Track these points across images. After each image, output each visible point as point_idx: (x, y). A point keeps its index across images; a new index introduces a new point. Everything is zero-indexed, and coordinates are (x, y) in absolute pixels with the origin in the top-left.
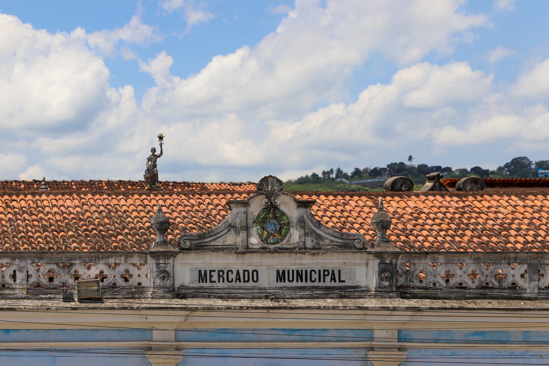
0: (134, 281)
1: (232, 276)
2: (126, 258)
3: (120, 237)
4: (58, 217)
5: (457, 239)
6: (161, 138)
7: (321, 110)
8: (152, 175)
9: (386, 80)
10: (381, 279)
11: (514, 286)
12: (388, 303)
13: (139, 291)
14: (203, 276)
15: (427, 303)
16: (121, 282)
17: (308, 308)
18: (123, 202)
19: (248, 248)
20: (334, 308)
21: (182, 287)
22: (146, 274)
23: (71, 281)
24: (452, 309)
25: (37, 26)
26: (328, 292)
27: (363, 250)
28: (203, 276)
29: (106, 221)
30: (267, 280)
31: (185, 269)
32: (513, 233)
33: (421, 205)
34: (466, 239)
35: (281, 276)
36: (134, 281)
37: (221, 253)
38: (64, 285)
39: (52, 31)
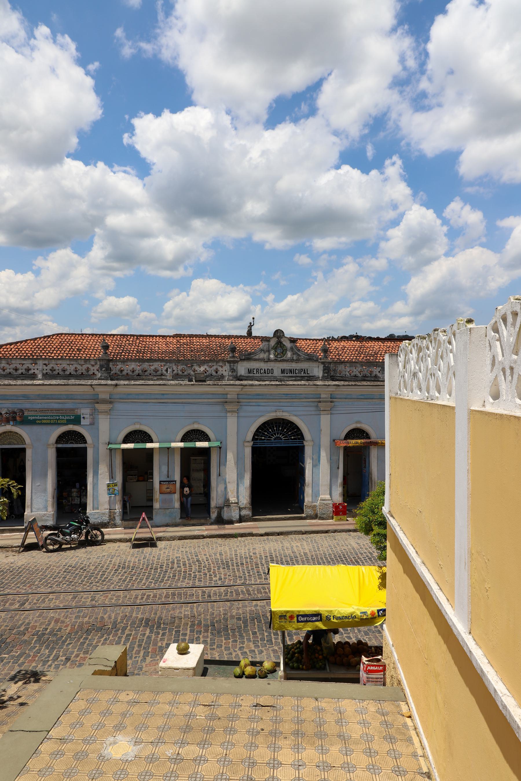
0: (220, 373)
1: (262, 371)
2: (217, 363)
3: (223, 355)
4: (198, 347)
5: (358, 358)
6: (253, 318)
7: (326, 315)
8: (250, 333)
9: (349, 306)
10: (324, 373)
11: (376, 376)
12: (327, 383)
13: (222, 377)
14: (250, 371)
15: (342, 383)
16: (214, 373)
17: (294, 385)
18: (227, 341)
19: (269, 359)
20: (304, 385)
21: (241, 376)
22: (225, 370)
23: (192, 373)
24: (352, 385)
25: (227, 284)
26: (302, 378)
27: (317, 361)
28: (250, 371)
29: (218, 348)
30: (277, 373)
31: (242, 369)
32: (379, 355)
33: (345, 345)
34: (361, 358)
35: (283, 371)
36: (220, 373)
37: (257, 362)
38: (189, 374)
39: (233, 286)
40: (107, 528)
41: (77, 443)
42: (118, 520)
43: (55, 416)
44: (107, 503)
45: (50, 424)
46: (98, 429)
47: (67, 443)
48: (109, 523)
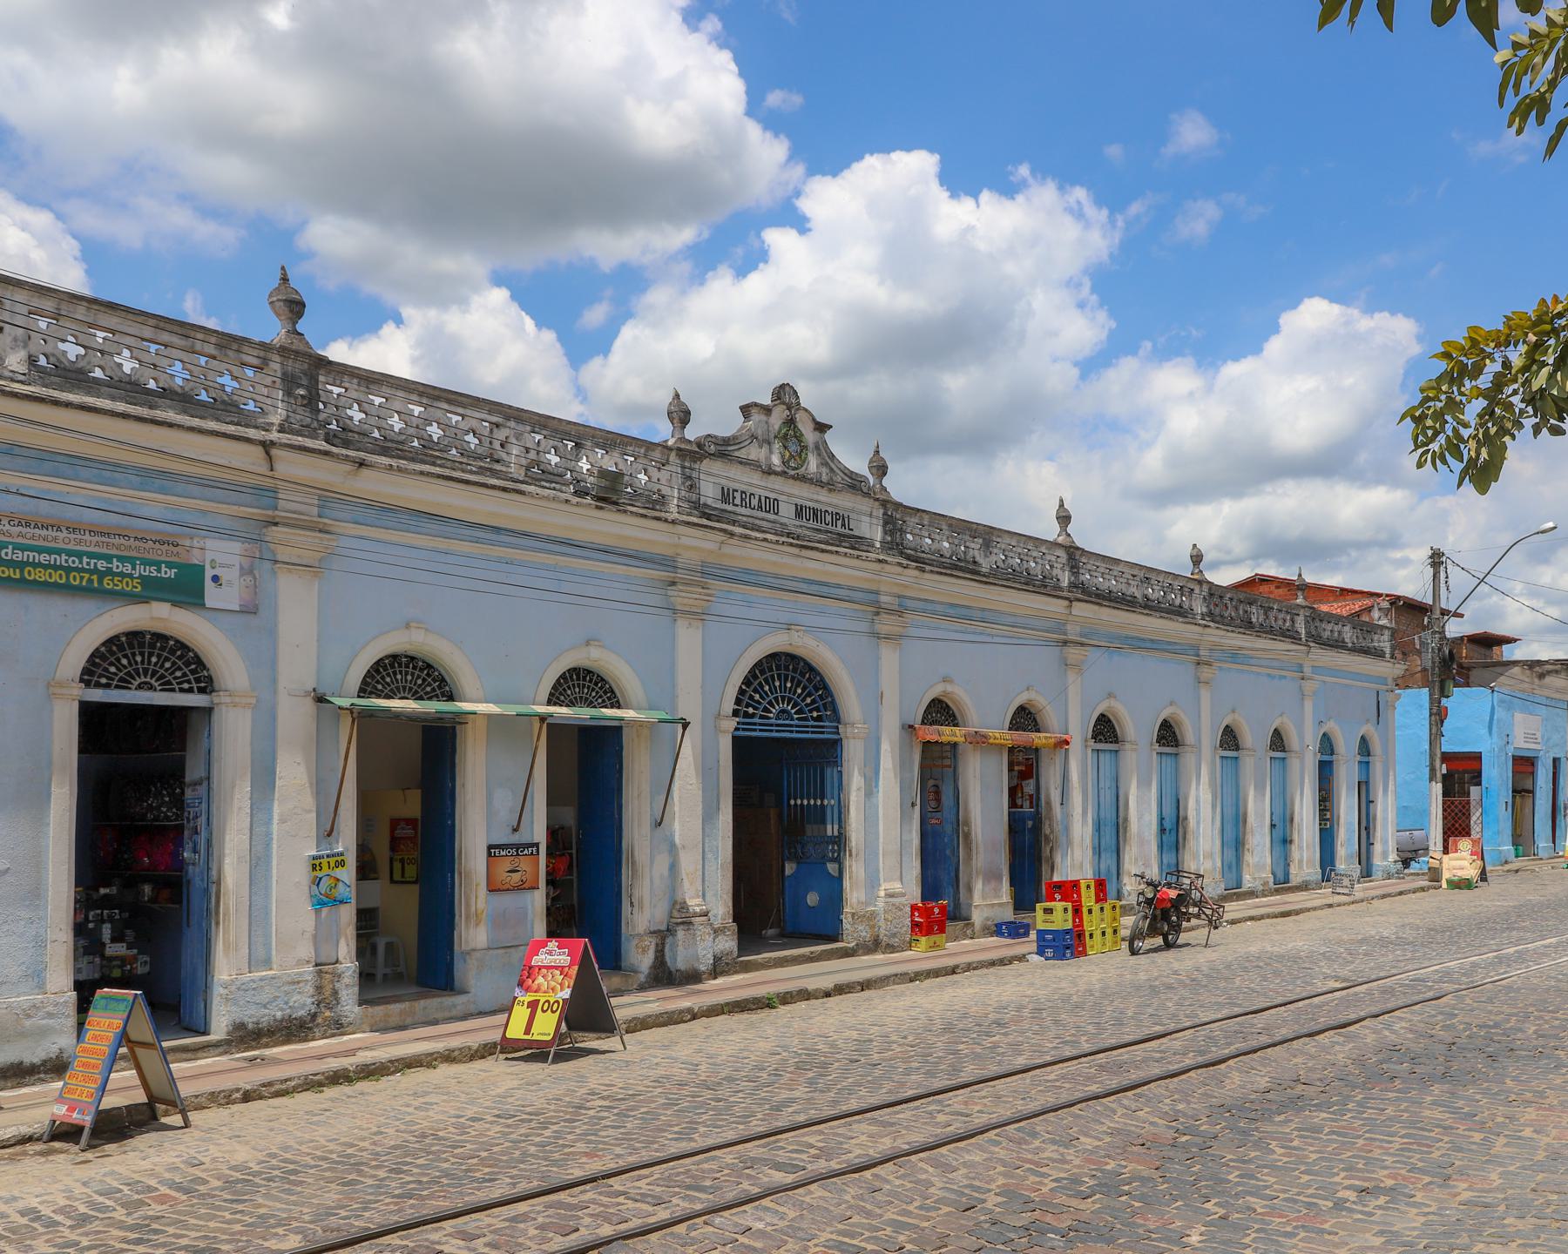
40: (306, 1040)
41: (167, 687)
42: (349, 1005)
43: (91, 555)
44: (308, 936)
45: (67, 589)
46: (272, 633)
47: (124, 684)
48: (314, 1016)
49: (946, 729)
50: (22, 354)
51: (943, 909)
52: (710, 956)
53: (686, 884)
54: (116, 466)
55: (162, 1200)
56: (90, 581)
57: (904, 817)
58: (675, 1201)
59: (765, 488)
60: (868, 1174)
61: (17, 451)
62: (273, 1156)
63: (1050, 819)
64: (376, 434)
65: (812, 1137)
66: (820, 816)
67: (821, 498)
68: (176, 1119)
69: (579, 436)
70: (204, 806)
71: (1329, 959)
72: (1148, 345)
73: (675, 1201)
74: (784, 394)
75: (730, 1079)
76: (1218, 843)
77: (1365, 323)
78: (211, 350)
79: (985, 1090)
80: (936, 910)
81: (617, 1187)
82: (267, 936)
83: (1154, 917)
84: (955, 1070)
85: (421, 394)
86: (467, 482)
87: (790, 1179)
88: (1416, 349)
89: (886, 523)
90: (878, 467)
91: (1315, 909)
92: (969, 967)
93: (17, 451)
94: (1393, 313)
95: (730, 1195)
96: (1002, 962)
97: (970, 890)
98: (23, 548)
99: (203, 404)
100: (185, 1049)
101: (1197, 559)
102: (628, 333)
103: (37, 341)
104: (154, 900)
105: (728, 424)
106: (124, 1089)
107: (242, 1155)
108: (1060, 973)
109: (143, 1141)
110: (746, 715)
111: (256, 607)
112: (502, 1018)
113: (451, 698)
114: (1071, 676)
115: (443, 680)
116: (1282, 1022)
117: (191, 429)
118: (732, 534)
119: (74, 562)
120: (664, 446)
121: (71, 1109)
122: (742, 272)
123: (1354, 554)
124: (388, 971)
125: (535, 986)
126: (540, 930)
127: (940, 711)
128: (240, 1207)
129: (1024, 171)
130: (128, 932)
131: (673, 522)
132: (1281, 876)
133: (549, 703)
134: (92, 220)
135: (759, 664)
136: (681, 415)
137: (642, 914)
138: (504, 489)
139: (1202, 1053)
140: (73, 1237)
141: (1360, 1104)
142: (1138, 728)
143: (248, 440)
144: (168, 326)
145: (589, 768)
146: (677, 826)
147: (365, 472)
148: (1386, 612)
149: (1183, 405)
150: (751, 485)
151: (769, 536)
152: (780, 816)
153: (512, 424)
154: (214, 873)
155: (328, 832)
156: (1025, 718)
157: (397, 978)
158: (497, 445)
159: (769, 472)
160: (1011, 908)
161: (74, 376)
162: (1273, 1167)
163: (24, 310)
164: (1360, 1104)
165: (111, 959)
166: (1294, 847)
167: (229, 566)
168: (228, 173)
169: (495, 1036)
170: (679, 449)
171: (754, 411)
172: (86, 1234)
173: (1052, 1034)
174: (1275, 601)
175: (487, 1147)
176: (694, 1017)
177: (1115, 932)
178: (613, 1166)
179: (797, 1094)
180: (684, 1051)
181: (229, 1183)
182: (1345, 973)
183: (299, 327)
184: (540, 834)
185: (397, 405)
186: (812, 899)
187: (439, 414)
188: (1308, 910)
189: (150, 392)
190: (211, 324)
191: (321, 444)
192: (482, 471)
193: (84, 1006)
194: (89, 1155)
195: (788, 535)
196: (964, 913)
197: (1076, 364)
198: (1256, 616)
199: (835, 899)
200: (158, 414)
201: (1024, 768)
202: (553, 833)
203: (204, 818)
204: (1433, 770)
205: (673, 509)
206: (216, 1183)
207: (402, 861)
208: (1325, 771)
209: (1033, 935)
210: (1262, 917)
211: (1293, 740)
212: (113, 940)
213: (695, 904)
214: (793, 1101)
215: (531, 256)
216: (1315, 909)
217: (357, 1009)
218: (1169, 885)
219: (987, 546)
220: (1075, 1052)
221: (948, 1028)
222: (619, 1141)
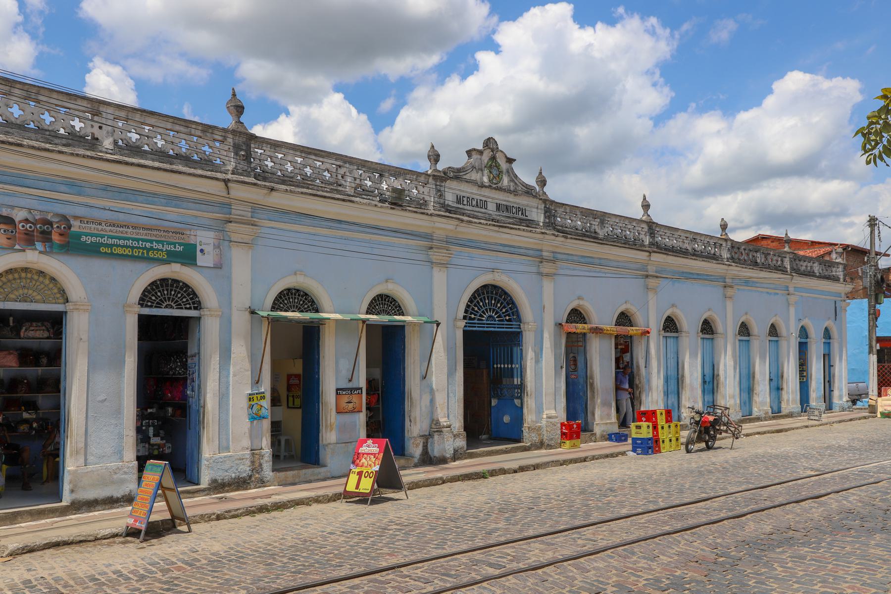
49: (580, 326)
50: (111, 140)
51: (578, 425)
52: (452, 449)
53: (439, 410)
54: (155, 195)
55: (179, 569)
56: (143, 253)
57: (557, 374)
58: (436, 581)
59: (480, 195)
60: (540, 571)
61: (109, 188)
62: (232, 548)
63: (639, 375)
64: (279, 174)
65: (508, 550)
66: (510, 373)
67: (511, 200)
68: (184, 528)
69: (381, 170)
70: (197, 367)
71: (807, 458)
72: (694, 105)
73: (436, 581)
74: (490, 143)
75: (463, 517)
76: (738, 390)
77: (826, 84)
78: (199, 133)
79: (604, 527)
80: (575, 426)
81: (405, 573)
82: (227, 435)
83: (700, 431)
84: (587, 515)
85: (302, 152)
86: (325, 197)
87: (497, 572)
88: (859, 98)
89: (546, 212)
90: (541, 181)
91: (797, 428)
92: (594, 458)
93: (109, 188)
94: (844, 78)
95: (465, 580)
96: (612, 455)
97: (593, 414)
98: (112, 238)
99: (195, 162)
100: (188, 492)
101: (724, 227)
102: (404, 113)
103: (118, 132)
104: (172, 416)
105: (459, 160)
106: (160, 512)
107: (217, 547)
108: (646, 462)
109: (169, 538)
110: (471, 319)
111: (221, 265)
112: (344, 480)
113: (317, 311)
114: (651, 295)
115: (313, 302)
116: (780, 494)
117: (190, 174)
118: (462, 221)
119: (135, 244)
120: (426, 174)
121: (136, 521)
122: (464, 77)
123: (819, 220)
124: (286, 454)
125: (361, 464)
126: (363, 434)
127: (576, 315)
128: (216, 574)
129: (621, 10)
130: (161, 432)
131: (431, 215)
132: (776, 409)
133: (367, 313)
134: (138, 69)
135: (477, 291)
136: (435, 157)
137: (415, 427)
138: (344, 200)
139: (730, 510)
140: (138, 586)
141: (829, 544)
142: (689, 324)
143: (217, 179)
144: (179, 122)
145: (387, 347)
146: (434, 379)
147: (274, 193)
148: (840, 254)
149: (714, 138)
150: (472, 193)
151: (482, 221)
152: (489, 374)
153: (347, 165)
154: (202, 402)
155: (257, 382)
156: (624, 319)
157: (290, 458)
158: (340, 177)
159: (482, 186)
160: (616, 426)
161: (134, 149)
162: (776, 578)
163: (112, 117)
164: (829, 544)
165: (153, 445)
166: (784, 392)
167: (208, 244)
168: (203, 41)
169: (341, 490)
170: (434, 176)
171: (473, 153)
172: (144, 585)
173: (641, 497)
174: (771, 249)
175: (338, 548)
176: (444, 482)
177: (677, 439)
178: (403, 561)
179: (500, 526)
180: (439, 501)
181: (211, 562)
182: (817, 466)
183: (242, 120)
184: (362, 383)
185: (290, 158)
186: (506, 419)
187: (310, 161)
188: (793, 429)
189: (170, 156)
190: (196, 119)
191: (252, 180)
192: (332, 191)
193: (141, 469)
194: (144, 545)
195: (492, 220)
196: (590, 428)
197: (651, 119)
198: (760, 258)
199: (519, 419)
200: (174, 167)
201: (624, 347)
202: (370, 382)
203: (197, 374)
204: (871, 347)
205: (431, 208)
206: (204, 562)
207: (293, 396)
208: (803, 348)
209: (630, 441)
210: (764, 433)
211: (783, 330)
212: (154, 436)
213: (443, 421)
214: (498, 529)
215: (354, 74)
216: (797, 428)
217: (271, 474)
218: (709, 413)
219: (602, 223)
220: (655, 507)
221: (583, 492)
222: (406, 548)
